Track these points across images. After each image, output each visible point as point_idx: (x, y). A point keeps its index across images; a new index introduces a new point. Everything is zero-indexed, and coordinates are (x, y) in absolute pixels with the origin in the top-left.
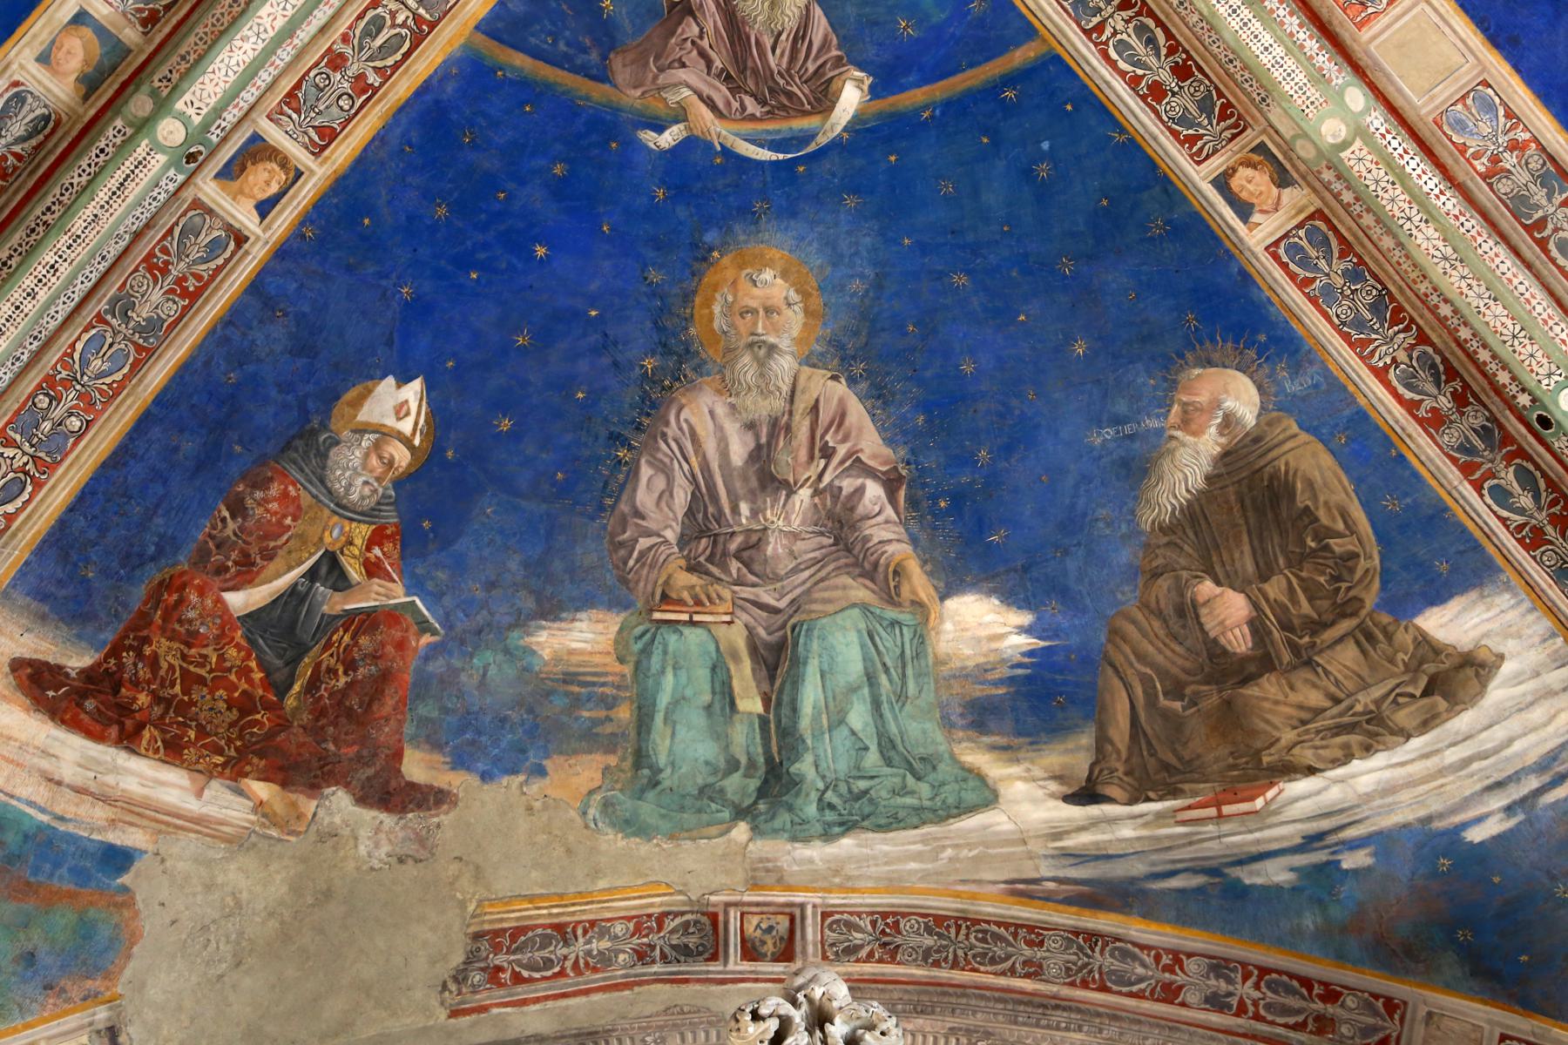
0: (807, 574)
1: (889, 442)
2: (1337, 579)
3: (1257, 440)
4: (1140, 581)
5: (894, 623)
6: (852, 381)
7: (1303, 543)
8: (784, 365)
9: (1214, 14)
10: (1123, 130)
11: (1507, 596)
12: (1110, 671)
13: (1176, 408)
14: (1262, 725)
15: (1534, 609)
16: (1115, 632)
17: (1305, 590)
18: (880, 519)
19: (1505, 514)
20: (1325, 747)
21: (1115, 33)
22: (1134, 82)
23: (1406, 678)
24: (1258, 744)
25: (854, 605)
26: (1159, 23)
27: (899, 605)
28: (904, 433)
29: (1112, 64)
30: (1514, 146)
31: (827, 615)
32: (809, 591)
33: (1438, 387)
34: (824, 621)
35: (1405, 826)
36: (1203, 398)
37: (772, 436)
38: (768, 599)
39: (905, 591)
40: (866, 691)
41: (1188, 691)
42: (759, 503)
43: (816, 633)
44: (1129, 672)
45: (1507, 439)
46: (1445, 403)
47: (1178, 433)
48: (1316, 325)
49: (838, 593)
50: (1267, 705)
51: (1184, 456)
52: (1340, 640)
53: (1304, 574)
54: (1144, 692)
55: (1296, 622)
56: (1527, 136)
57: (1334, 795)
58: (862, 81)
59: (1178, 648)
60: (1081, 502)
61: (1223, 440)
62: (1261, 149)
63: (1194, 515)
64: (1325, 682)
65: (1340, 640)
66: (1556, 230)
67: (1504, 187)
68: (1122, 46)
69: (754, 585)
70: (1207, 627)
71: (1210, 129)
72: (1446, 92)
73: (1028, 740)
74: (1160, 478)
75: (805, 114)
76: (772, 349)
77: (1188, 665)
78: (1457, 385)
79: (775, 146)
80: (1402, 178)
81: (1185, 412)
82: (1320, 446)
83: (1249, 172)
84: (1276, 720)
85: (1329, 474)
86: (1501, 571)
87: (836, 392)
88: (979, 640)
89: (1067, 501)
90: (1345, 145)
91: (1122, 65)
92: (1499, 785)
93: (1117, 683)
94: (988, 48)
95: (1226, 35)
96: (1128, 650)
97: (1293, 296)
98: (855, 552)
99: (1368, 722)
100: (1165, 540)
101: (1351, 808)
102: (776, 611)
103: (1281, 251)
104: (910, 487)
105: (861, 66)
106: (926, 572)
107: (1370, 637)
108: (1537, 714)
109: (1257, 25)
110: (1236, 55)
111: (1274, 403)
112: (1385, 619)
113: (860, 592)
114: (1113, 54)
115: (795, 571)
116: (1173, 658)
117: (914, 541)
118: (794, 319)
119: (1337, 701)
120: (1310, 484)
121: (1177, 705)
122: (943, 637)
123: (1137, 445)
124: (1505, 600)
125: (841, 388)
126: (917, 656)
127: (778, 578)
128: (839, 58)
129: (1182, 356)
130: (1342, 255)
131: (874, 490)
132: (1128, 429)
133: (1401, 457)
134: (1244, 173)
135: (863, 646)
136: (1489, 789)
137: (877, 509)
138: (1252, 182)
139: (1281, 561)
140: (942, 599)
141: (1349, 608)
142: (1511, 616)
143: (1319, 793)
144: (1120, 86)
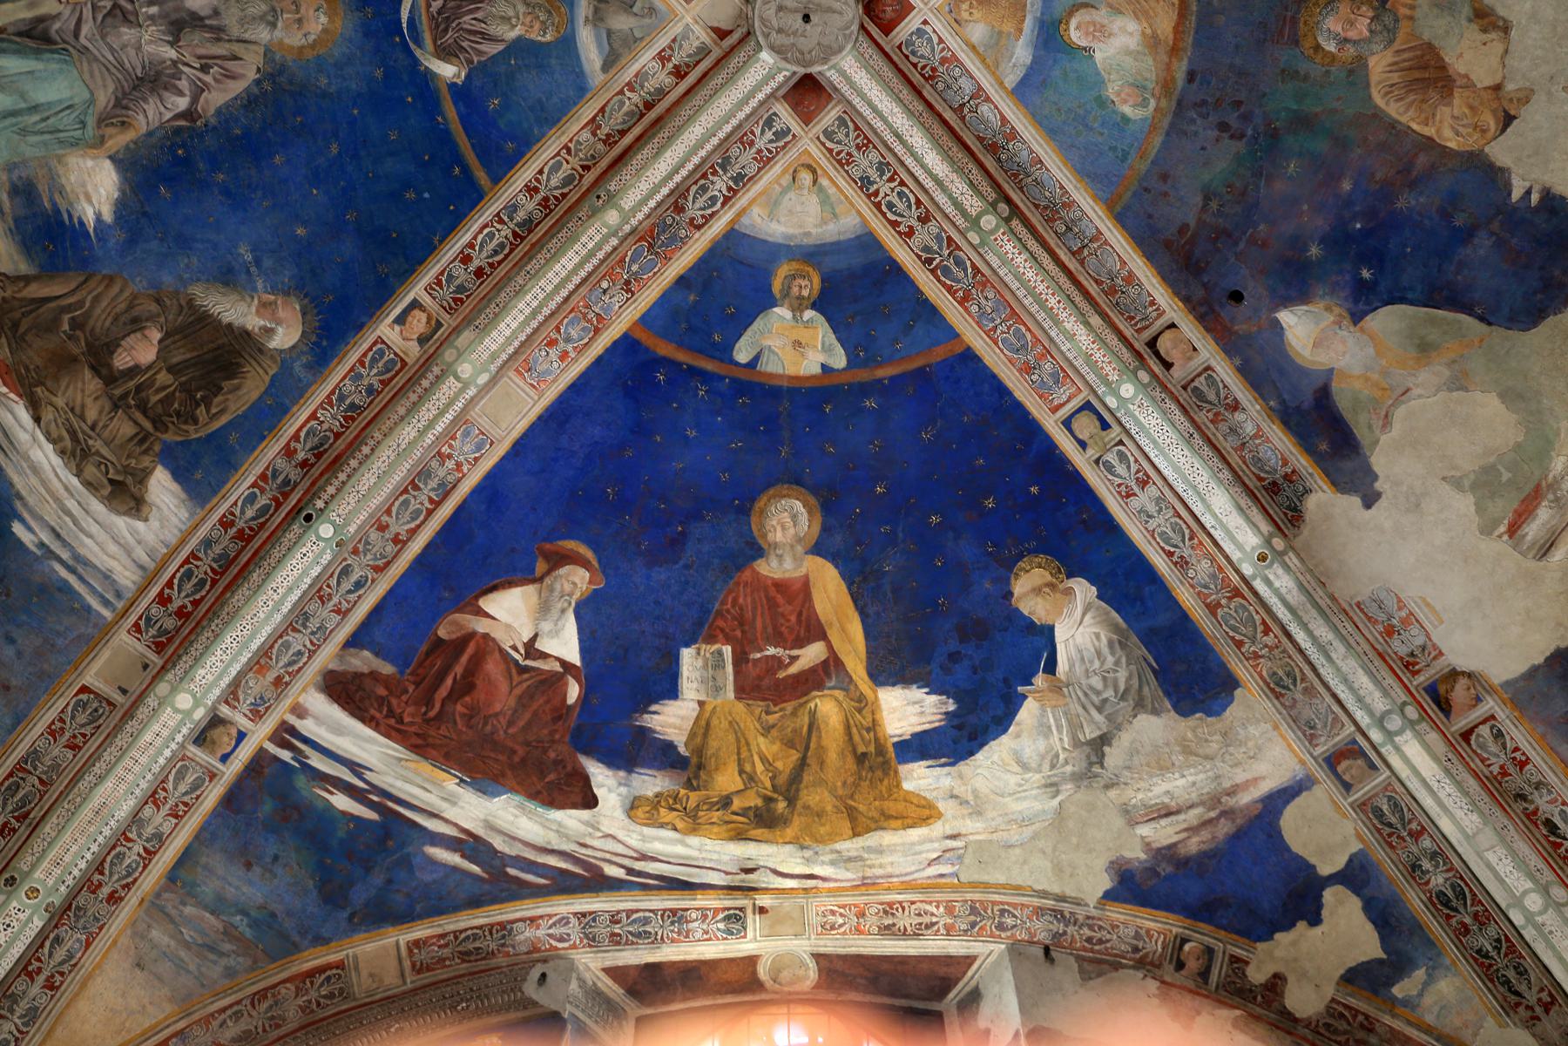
0: (111, 58)
1: (219, 112)
2: (178, 414)
3: (260, 351)
4: (151, 292)
5: (83, 124)
6: (258, 82)
7: (199, 389)
8: (263, 34)
9: (526, 293)
10: (441, 242)
11: (186, 515)
12: (82, 279)
13: (272, 298)
14: (64, 384)
15: (181, 531)
16: (111, 280)
17: (166, 396)
18: (162, 109)
19: (240, 504)
20: (57, 425)
21: (498, 230)
22: (471, 245)
23: (119, 467)
24: (49, 383)
25: (92, 94)
26: (507, 256)
27: (99, 127)
28: (227, 121)
29: (481, 231)
30: (459, 465)
31: (81, 74)
32: (96, 59)
33: (311, 449)
34: (75, 72)
35: (12, 485)
36: (281, 313)
37: (211, 29)
38: (86, 29)
39: (110, 131)
40: (23, 105)
41: (78, 333)
42: (160, 21)
43: (64, 66)
44: (84, 293)
45: (286, 495)
46: (301, 456)
47: (256, 301)
48: (336, 375)
49: (99, 80)
50: (80, 385)
51: (242, 307)
52: (136, 423)
53: (177, 394)
54: (70, 305)
55: (144, 394)
56: (465, 470)
57: (23, 437)
58: (459, 76)
59: (107, 323)
60: (199, 246)
61: (256, 330)
62: (439, 325)
63: (203, 321)
64: (104, 419)
65: (136, 423)
66: (415, 497)
67: (434, 464)
68: (491, 236)
69: (94, 18)
70: (128, 339)
71: (447, 293)
72: (485, 423)
73: (13, 227)
74: (224, 294)
75: (435, 42)
76: (273, 25)
77: (98, 330)
78: (313, 460)
79: (411, 21)
80: (442, 413)
81: (270, 304)
82: (263, 389)
83: (424, 320)
84: (70, 392)
85: (246, 398)
86: (203, 508)
87: (249, 71)
88: (84, 185)
89: (199, 236)
90: (457, 378)
91: (480, 237)
92: (58, 536)
93: (73, 285)
94: (484, 155)
95: (513, 302)
96: (100, 290)
97: (353, 358)
98: (134, 93)
99: (82, 449)
100: (183, 303)
101: (15, 448)
102: (76, 35)
103: (379, 346)
104: (188, 128)
105: (468, 76)
106: (127, 145)
107: (142, 442)
108: (113, 548)
109: (521, 318)
110: (504, 309)
111: (285, 358)
112: (157, 448)
113: (104, 98)
114: (485, 231)
115: (112, 50)
116: (101, 319)
117: (150, 134)
118: (295, 40)
119: (93, 428)
120: (238, 388)
121: (66, 327)
122: (81, 161)
123: (244, 276)
124: (184, 514)
125: (252, 75)
126: (61, 142)
127: (103, 37)
128: (472, 62)
129: (306, 296)
130: (382, 382)
131: (182, 103)
132: (253, 269)
133: (264, 437)
134: (424, 317)
135: (60, 101)
136: (53, 530)
137: (169, 106)
138: (418, 322)
139: (183, 379)
140: (110, 157)
141: (159, 424)
142: (174, 520)
143: (21, 427)
144: (467, 238)
